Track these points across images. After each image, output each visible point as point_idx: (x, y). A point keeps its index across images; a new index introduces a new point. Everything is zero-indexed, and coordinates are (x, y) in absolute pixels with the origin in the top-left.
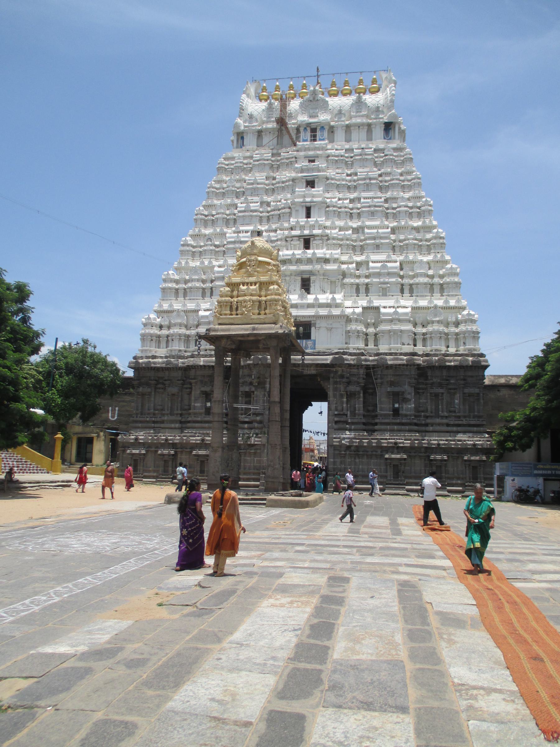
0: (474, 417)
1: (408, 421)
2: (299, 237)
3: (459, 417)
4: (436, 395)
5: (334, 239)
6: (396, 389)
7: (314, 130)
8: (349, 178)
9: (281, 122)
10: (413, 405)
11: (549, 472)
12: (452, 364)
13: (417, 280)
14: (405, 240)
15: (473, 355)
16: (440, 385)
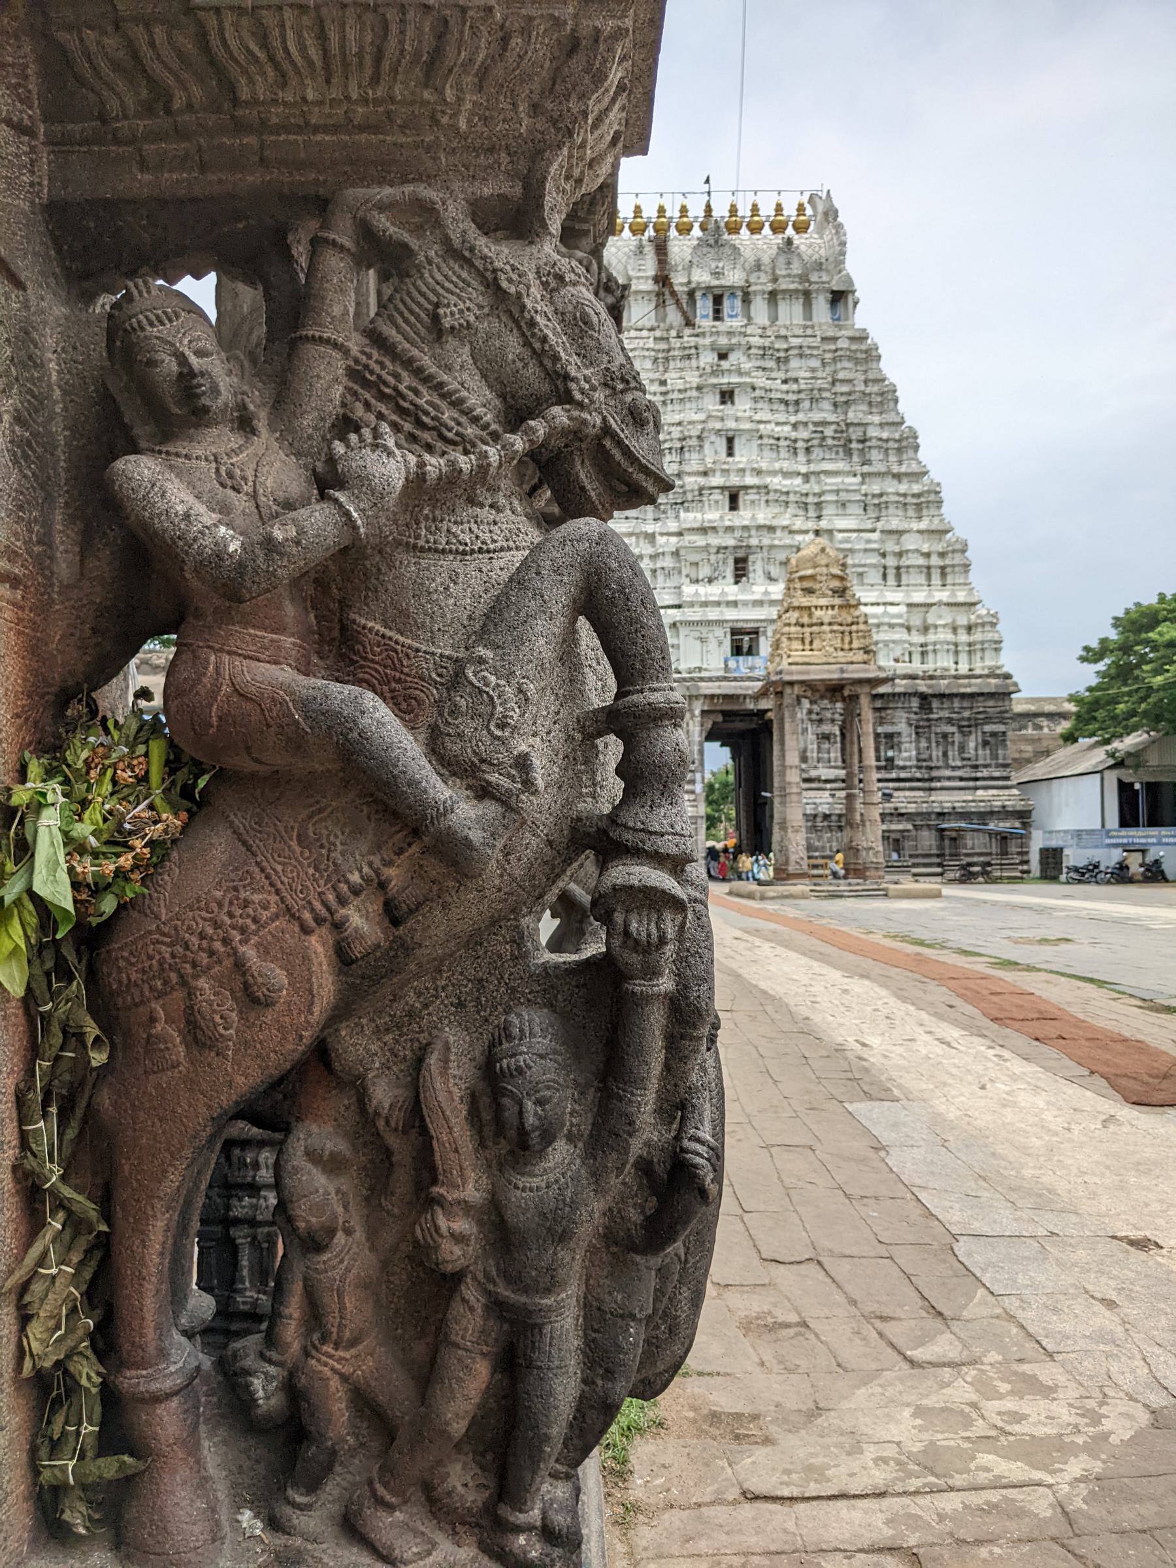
0: (998, 766)
1: (908, 775)
2: (723, 488)
3: (976, 767)
4: (945, 736)
5: (776, 491)
6: (889, 729)
7: (718, 300)
8: (785, 387)
9: (663, 280)
10: (914, 753)
11: (1125, 841)
12: (968, 690)
13: (905, 562)
14: (881, 495)
15: (998, 676)
16: (950, 721)
